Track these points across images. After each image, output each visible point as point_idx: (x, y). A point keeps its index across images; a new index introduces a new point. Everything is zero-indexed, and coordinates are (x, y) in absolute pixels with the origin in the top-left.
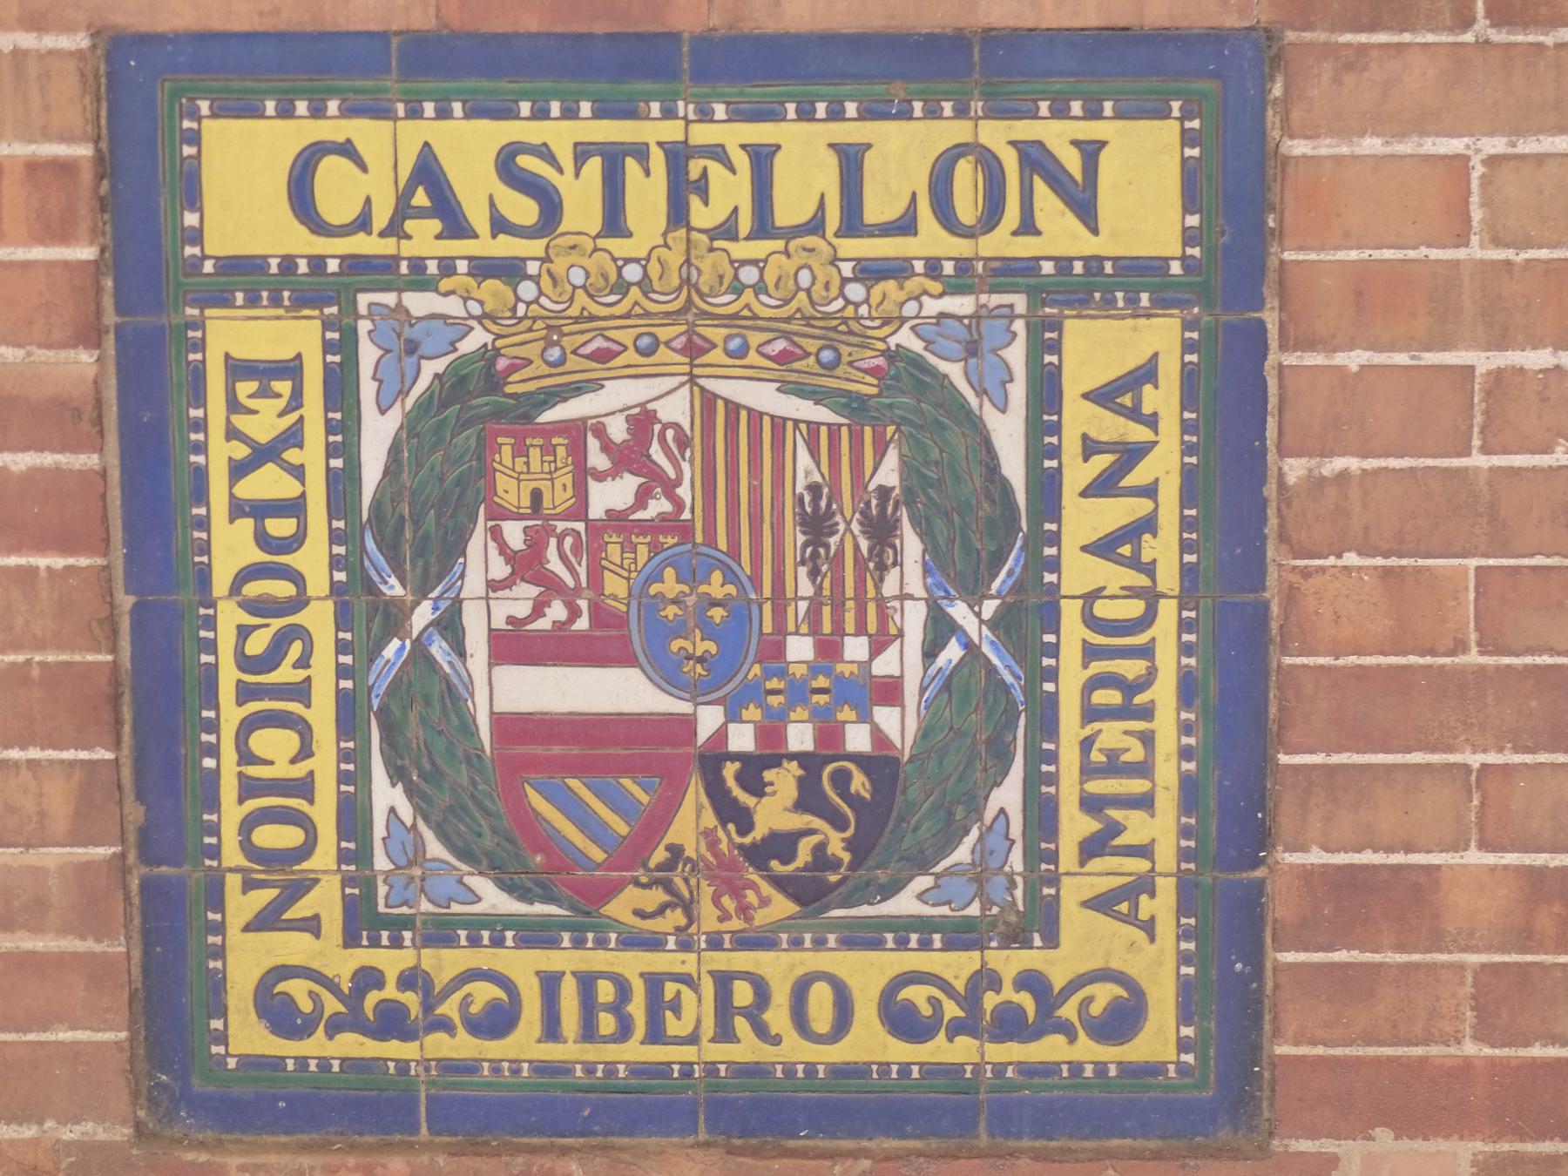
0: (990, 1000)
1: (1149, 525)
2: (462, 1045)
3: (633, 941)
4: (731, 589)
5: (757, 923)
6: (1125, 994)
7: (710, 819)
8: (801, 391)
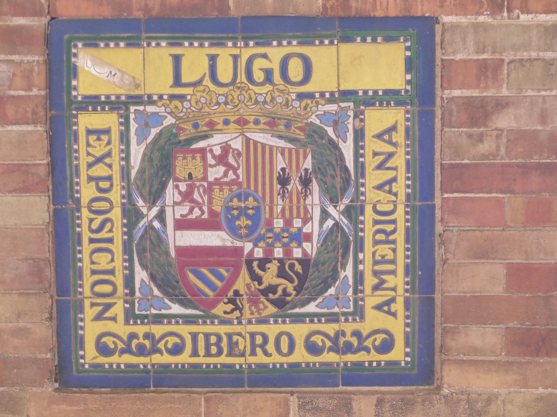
0: (342, 340)
2: (166, 359)
3: (223, 322)
4: (255, 203)
5: (262, 315)
7: (248, 280)
8: (280, 137)
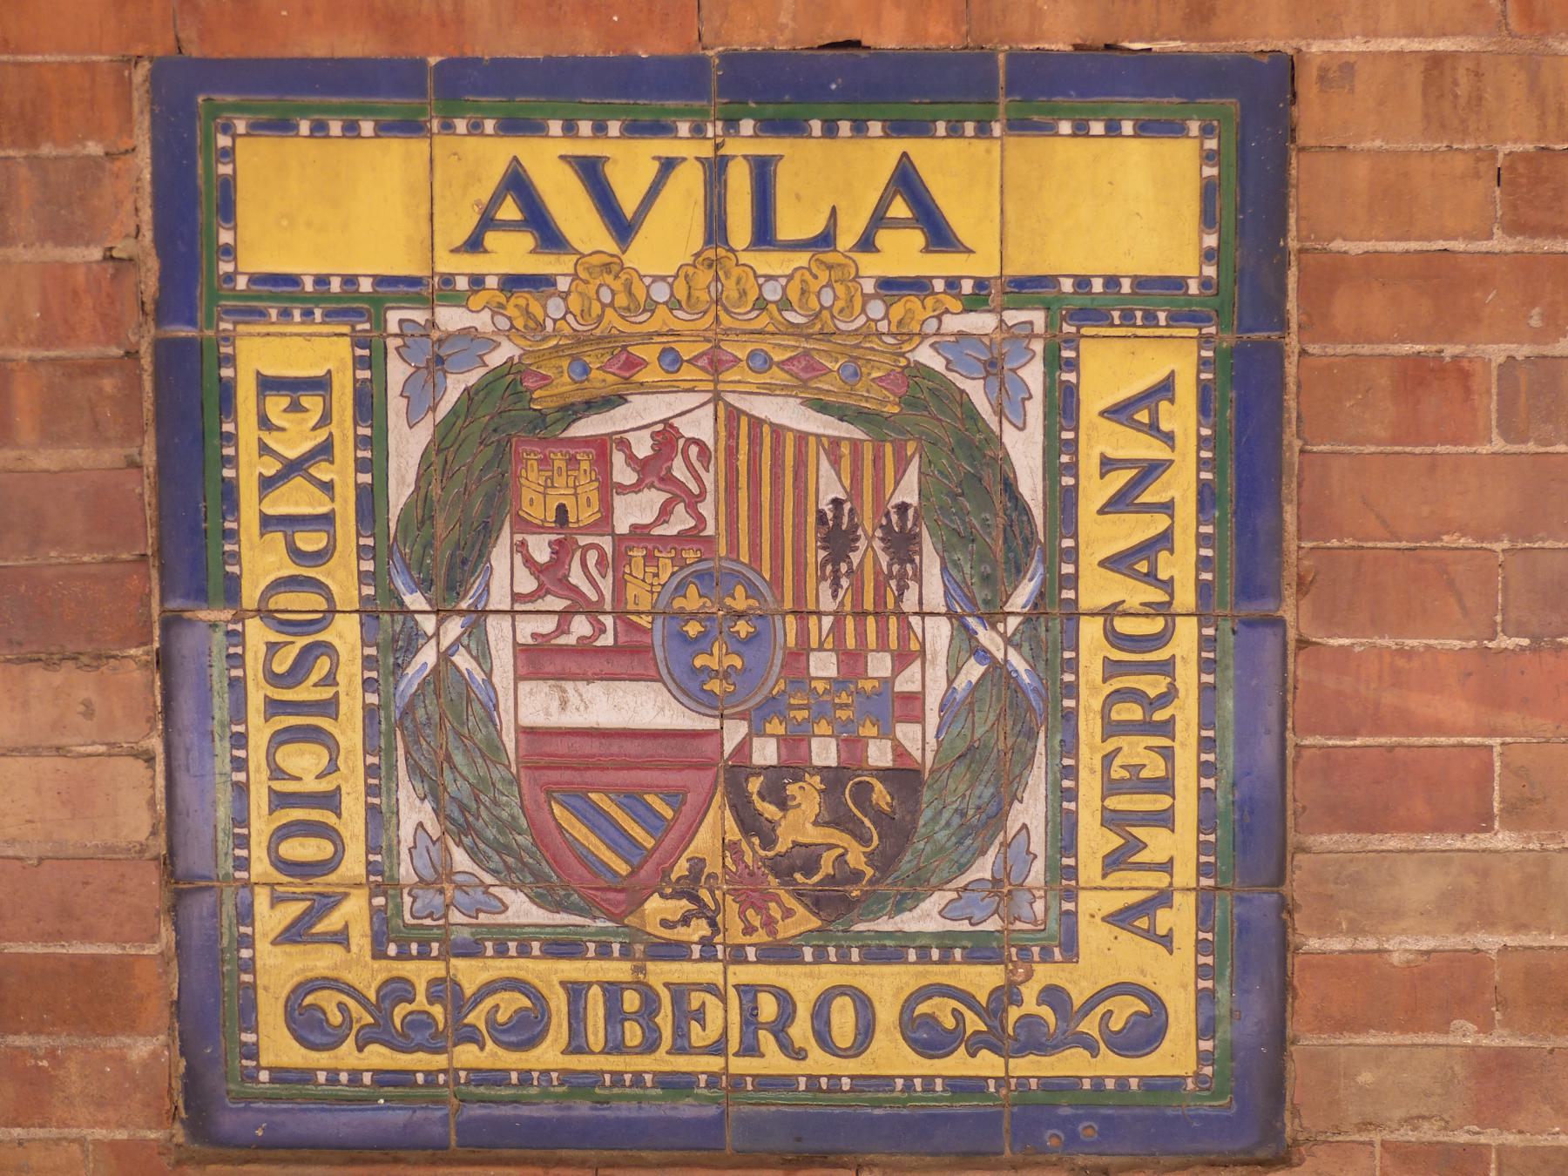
1: (1164, 540)
2: (490, 1056)
5: (780, 936)
6: (1144, 1008)
8: (822, 407)
